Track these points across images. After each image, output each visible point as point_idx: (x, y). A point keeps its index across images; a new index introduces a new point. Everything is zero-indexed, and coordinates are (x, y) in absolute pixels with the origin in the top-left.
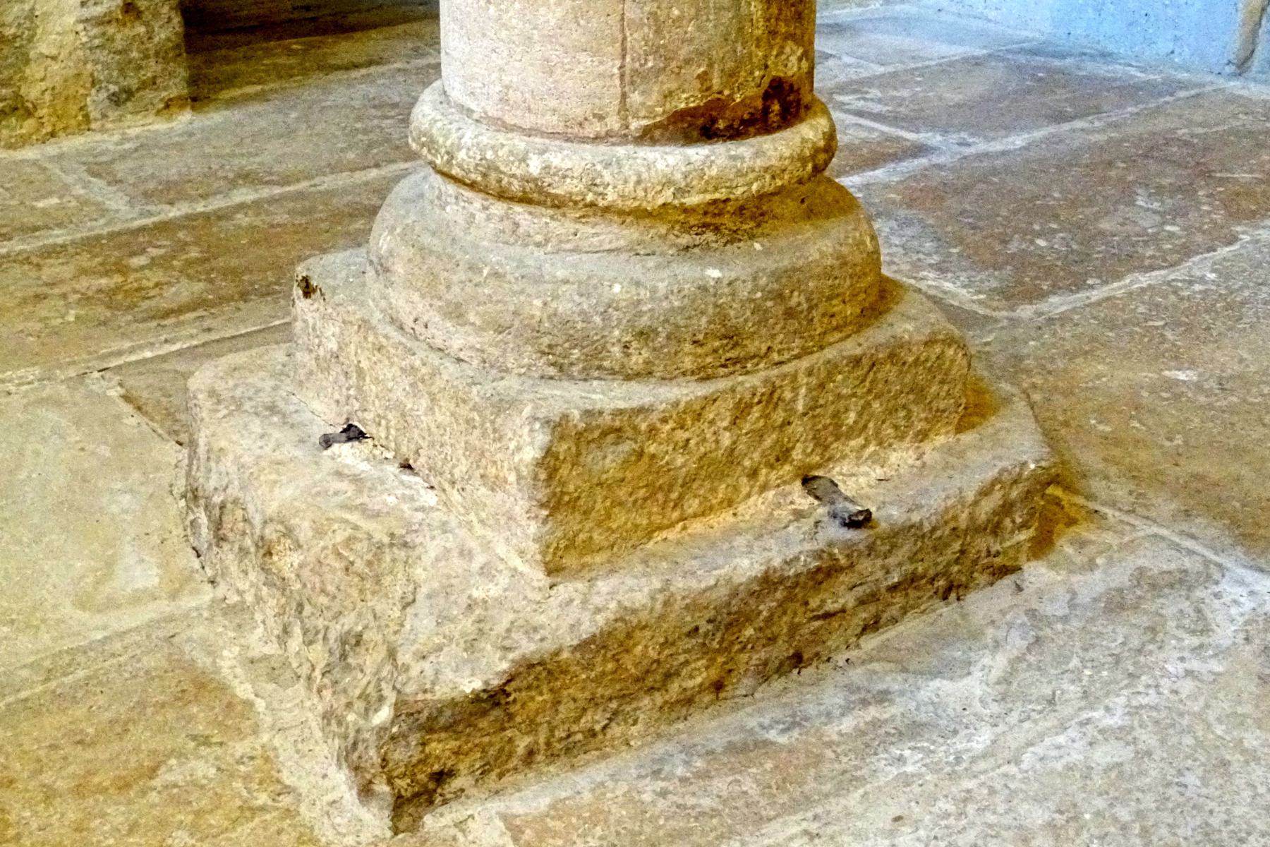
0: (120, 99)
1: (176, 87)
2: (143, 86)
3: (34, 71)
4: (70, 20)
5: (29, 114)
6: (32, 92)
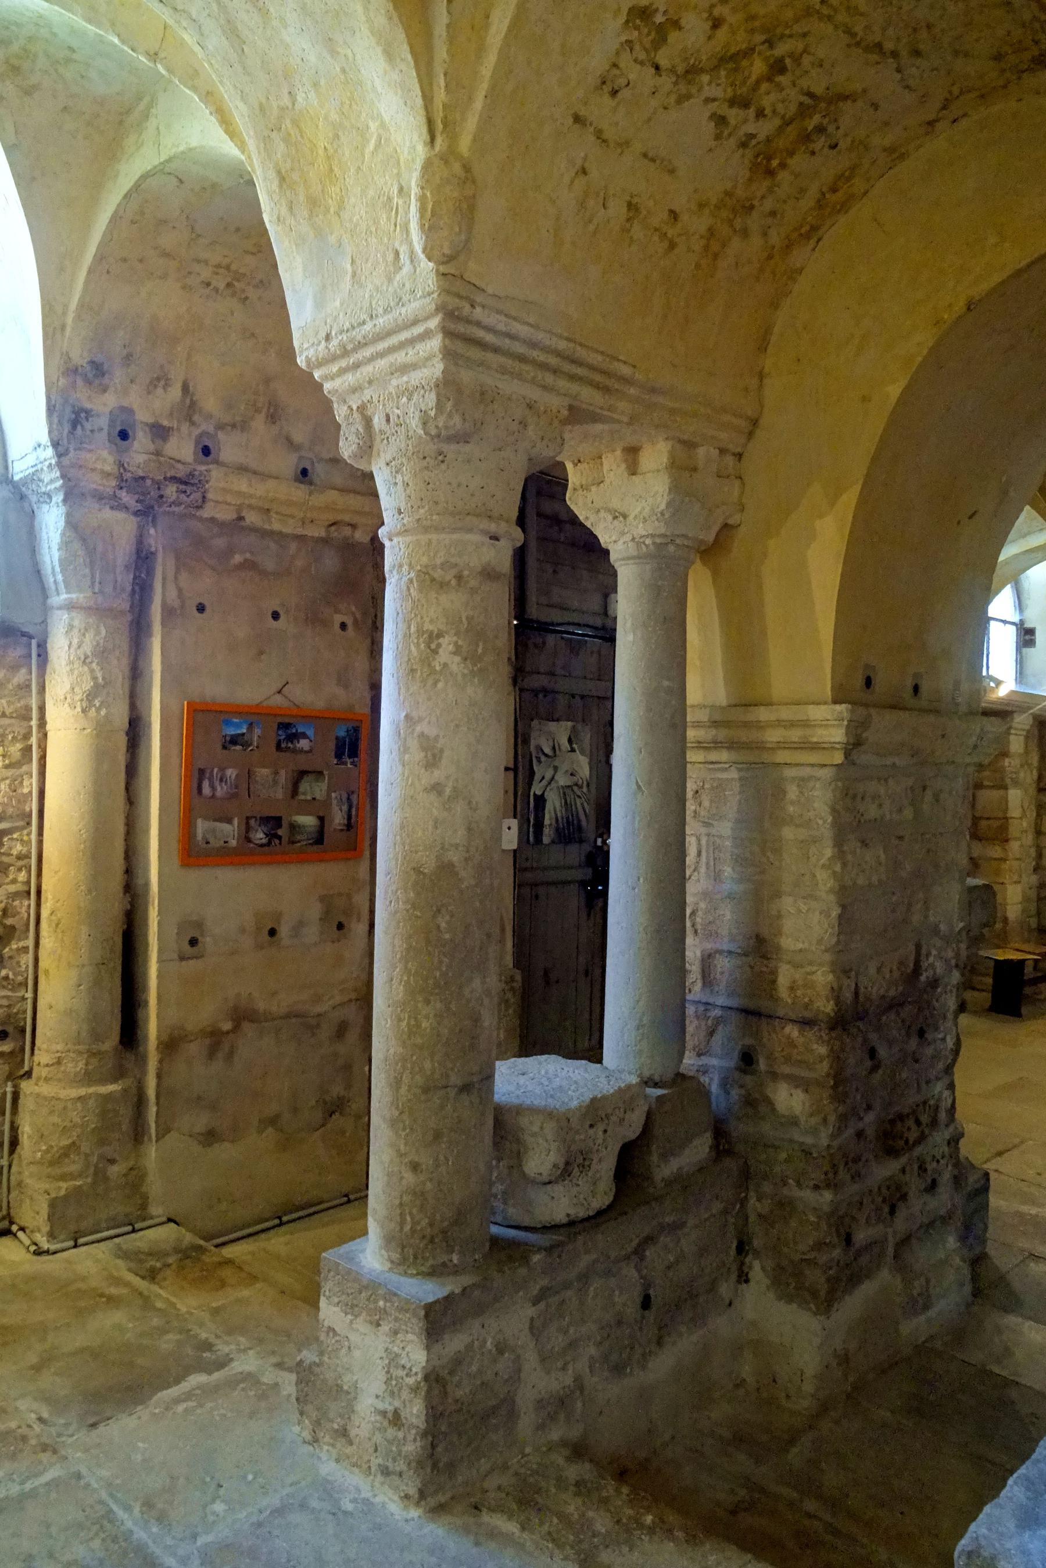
0: (386, 1472)
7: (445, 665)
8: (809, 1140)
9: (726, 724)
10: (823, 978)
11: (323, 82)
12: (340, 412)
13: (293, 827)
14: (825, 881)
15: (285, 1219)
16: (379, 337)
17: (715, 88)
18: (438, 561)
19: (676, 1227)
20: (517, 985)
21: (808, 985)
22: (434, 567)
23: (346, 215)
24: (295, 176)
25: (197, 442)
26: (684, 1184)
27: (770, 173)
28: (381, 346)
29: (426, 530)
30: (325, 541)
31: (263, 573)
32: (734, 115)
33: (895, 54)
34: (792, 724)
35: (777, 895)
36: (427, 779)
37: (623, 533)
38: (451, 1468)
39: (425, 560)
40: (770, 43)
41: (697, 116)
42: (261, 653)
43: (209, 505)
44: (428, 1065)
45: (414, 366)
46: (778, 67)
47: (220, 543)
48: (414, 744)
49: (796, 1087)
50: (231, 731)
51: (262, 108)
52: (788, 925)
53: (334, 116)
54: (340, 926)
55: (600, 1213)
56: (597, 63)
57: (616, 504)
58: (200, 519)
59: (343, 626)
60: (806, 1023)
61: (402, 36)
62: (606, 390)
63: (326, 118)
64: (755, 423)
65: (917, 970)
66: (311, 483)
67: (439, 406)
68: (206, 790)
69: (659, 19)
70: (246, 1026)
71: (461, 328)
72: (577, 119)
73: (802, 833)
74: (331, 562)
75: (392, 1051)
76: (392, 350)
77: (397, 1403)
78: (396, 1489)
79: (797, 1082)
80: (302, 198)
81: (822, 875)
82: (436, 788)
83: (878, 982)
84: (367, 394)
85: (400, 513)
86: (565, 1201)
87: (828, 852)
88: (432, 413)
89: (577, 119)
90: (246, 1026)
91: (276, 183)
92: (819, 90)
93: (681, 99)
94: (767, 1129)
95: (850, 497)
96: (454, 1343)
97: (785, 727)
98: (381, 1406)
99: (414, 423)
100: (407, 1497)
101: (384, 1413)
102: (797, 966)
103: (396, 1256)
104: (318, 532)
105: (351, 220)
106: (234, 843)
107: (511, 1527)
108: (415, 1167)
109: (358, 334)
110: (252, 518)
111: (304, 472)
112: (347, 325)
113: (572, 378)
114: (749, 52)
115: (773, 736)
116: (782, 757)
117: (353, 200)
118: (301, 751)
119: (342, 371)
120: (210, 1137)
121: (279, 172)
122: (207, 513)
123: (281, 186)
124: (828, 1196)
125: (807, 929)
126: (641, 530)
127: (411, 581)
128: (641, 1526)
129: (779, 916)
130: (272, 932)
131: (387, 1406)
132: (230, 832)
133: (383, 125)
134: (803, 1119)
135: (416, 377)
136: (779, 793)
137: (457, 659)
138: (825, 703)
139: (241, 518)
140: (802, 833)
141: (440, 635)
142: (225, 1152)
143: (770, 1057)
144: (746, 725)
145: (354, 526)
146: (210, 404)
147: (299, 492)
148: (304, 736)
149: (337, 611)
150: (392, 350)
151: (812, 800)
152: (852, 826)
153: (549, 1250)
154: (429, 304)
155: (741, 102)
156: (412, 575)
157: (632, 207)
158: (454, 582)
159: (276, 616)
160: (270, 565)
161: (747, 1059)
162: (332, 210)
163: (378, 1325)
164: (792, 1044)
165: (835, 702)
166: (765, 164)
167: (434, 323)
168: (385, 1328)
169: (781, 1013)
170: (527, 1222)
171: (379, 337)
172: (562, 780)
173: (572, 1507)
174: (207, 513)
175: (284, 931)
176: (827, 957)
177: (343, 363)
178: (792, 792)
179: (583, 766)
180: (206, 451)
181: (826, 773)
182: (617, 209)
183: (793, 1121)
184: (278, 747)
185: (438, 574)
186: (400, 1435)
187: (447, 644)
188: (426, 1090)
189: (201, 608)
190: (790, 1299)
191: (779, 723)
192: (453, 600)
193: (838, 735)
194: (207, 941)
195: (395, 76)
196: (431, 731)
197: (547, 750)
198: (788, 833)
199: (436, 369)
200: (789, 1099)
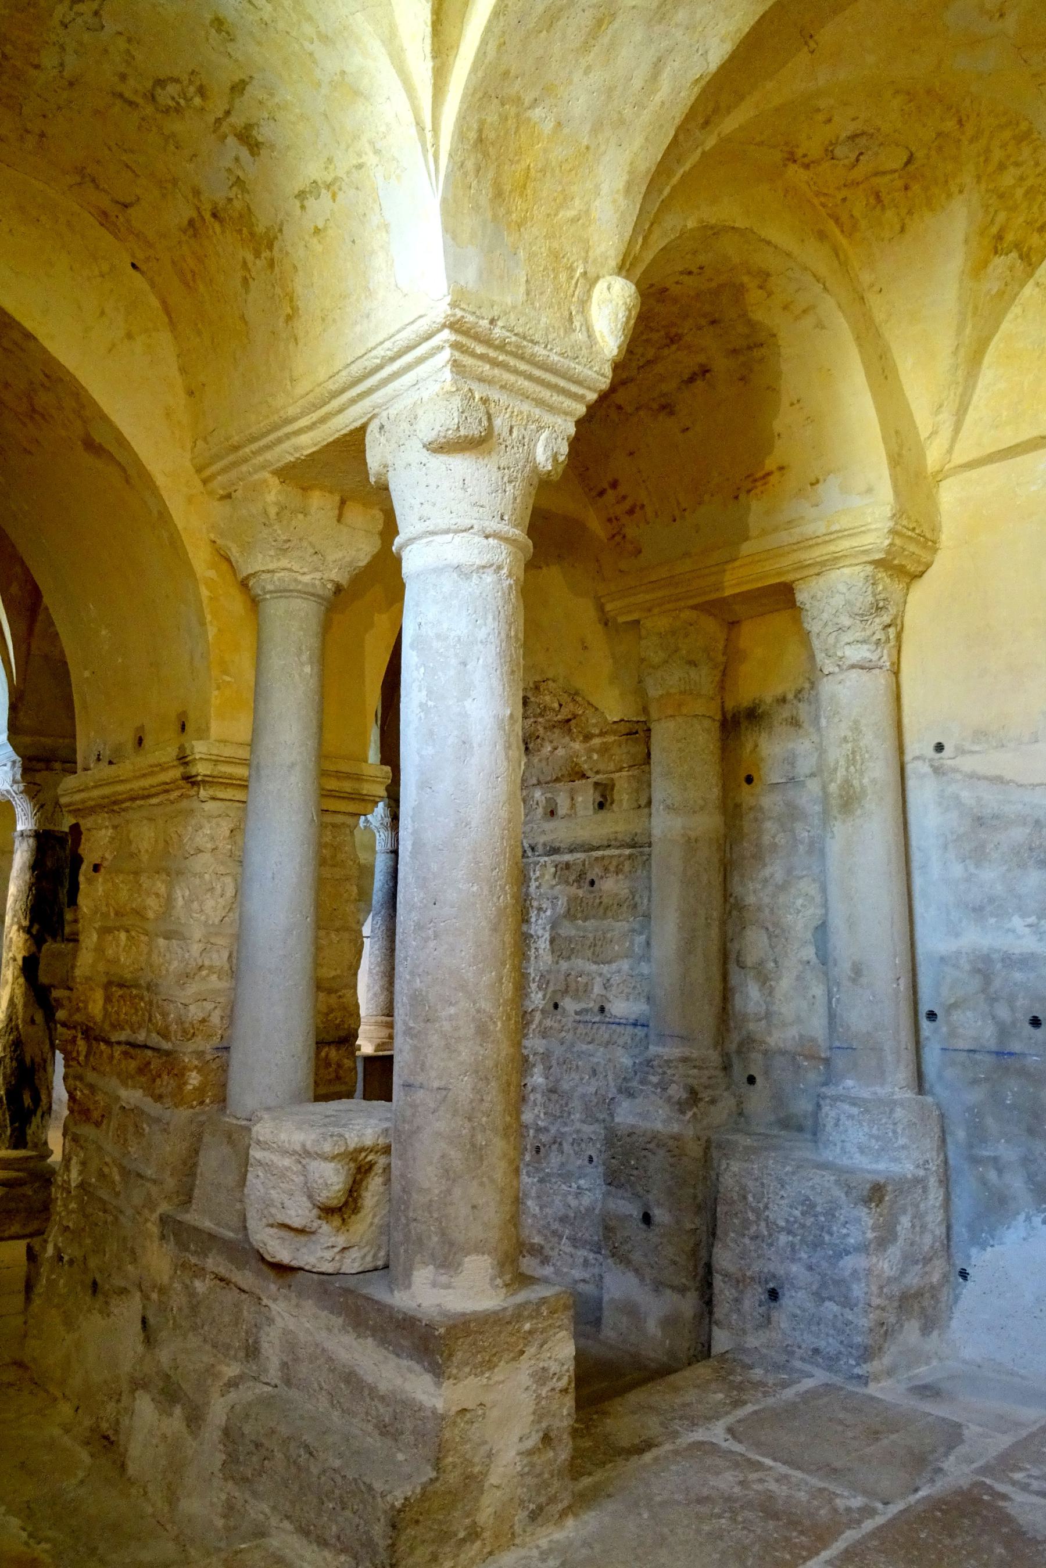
11: (566, 131)
34: (348, 776)
37: (317, 570)
51: (506, 74)
63: (545, 151)
75: (503, 1054)
84: (494, 394)
91: (473, 135)
97: (338, 778)
101: (530, 1453)
109: (530, 349)
117: (535, 231)
119: (482, 357)
121: (480, 131)
127: (510, 586)
133: (587, 212)
163: (522, 1352)
177: (492, 354)
195: (622, 202)
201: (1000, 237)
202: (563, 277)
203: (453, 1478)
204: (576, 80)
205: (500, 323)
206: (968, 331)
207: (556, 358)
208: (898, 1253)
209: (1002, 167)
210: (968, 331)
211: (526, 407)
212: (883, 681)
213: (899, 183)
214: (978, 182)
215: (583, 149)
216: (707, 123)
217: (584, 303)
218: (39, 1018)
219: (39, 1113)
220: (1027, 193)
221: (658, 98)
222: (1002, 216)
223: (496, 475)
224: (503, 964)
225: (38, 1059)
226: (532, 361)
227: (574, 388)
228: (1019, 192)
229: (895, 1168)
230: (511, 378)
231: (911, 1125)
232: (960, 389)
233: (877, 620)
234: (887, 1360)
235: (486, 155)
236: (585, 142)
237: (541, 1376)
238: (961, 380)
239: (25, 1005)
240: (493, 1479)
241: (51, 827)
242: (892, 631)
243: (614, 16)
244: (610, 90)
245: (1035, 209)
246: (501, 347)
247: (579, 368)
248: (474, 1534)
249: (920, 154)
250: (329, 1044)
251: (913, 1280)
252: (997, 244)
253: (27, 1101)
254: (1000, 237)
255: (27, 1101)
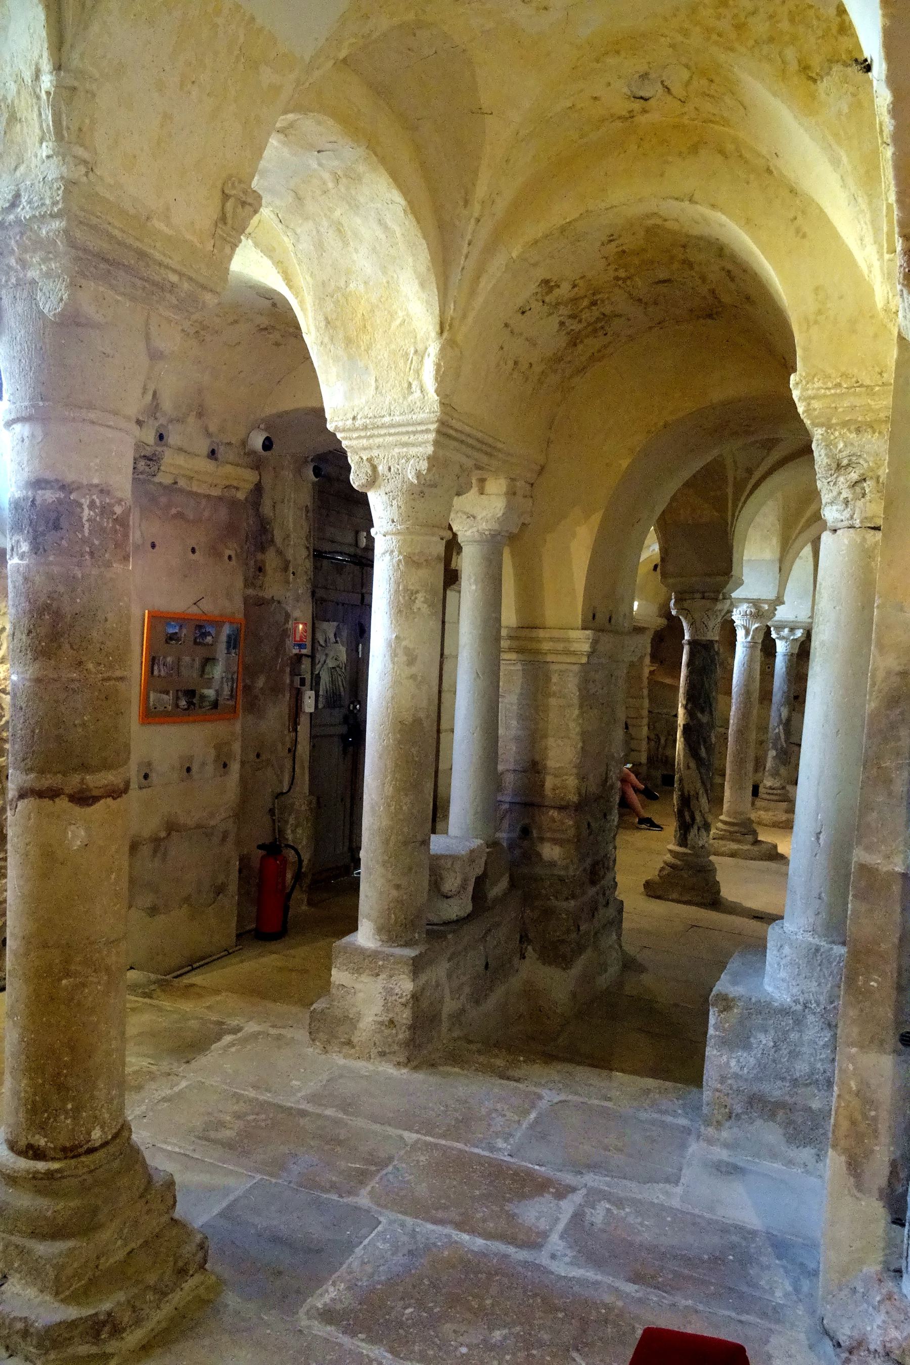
0: (382, 1054)
1: (402, 1059)
2: (389, 1053)
3: (357, 1033)
4: (371, 1019)
5: (353, 1047)
6: (355, 1040)
7: (419, 609)
8: (562, 873)
9: (517, 638)
10: (572, 782)
11: (371, 283)
12: (352, 460)
13: (203, 697)
14: (574, 729)
15: (195, 966)
16: (392, 426)
17: (564, 311)
18: (417, 551)
19: (498, 925)
20: (314, 805)
21: (565, 787)
22: (414, 554)
23: (373, 353)
24: (338, 323)
25: (157, 431)
26: (501, 900)
27: (575, 345)
28: (392, 431)
29: (411, 533)
30: (220, 498)
31: (188, 521)
32: (568, 322)
33: (646, 303)
35: (545, 736)
36: (408, 671)
38: (419, 1047)
39: (409, 550)
40: (594, 294)
41: (554, 321)
42: (186, 576)
43: (160, 474)
44: (406, 830)
45: (413, 445)
46: (594, 303)
47: (163, 500)
48: (400, 652)
49: (555, 844)
50: (171, 631)
51: (323, 283)
52: (551, 754)
53: (374, 300)
54: (225, 765)
55: (469, 915)
56: (520, 301)
57: (468, 509)
58: (154, 484)
59: (230, 558)
60: (561, 808)
61: (433, 278)
62: (490, 455)
64: (543, 468)
65: (606, 781)
66: (216, 459)
67: (429, 470)
68: (156, 673)
69: (552, 284)
70: (174, 833)
71: (445, 430)
72: (506, 325)
73: (562, 702)
74: (223, 514)
76: (398, 434)
77: (391, 1016)
78: (390, 1061)
79: (555, 841)
80: (341, 336)
81: (572, 725)
82: (413, 677)
83: (593, 787)
84: (375, 453)
85: (393, 521)
86: (456, 908)
87: (577, 712)
88: (424, 473)
89: (506, 325)
90: (174, 833)
91: (323, 324)
92: (607, 312)
93: (550, 314)
94: (539, 870)
95: (596, 518)
96: (423, 978)
98: (380, 1019)
99: (411, 476)
100: (399, 1063)
102: (556, 776)
103: (385, 938)
104: (216, 492)
105: (376, 357)
106: (170, 708)
107: (457, 1070)
108: (398, 887)
109: (379, 422)
110: (182, 483)
111: (213, 452)
112: (371, 415)
113: (479, 450)
114: (582, 298)
115: (546, 646)
116: (549, 658)
117: (379, 346)
118: (208, 644)
120: (153, 911)
121: (326, 319)
122: (156, 479)
123: (326, 326)
124: (573, 903)
125: (562, 756)
126: (484, 526)
127: (400, 561)
128: (519, 1061)
129: (546, 748)
130: (189, 770)
131: (385, 1018)
132: (168, 699)
133: (408, 315)
134: (559, 863)
135: (413, 451)
136: (548, 679)
137: (426, 606)
138: (578, 629)
139: (176, 483)
140: (562, 702)
141: (417, 592)
142: (161, 919)
143: (540, 828)
144: (532, 639)
145: (237, 489)
146: (167, 405)
147: (208, 466)
148: (209, 634)
149: (227, 548)
150: (398, 434)
151: (566, 684)
152: (587, 699)
153: (454, 932)
154: (433, 417)
155: (573, 317)
156: (401, 557)
157: (516, 363)
158: (425, 563)
159: (193, 551)
160: (191, 516)
161: (525, 832)
162: (362, 348)
164: (553, 820)
165: (584, 628)
166: (574, 341)
167: (433, 427)
168: (383, 976)
169: (546, 804)
170: (436, 921)
171: (392, 426)
172: (331, 664)
173: (481, 1059)
174: (156, 479)
175: (195, 769)
176: (575, 771)
177: (363, 434)
178: (555, 679)
179: (342, 652)
180: (161, 437)
181: (576, 668)
182: (511, 363)
183: (553, 864)
184: (195, 643)
185: (415, 558)
186: (394, 1031)
187: (420, 597)
188: (405, 843)
189: (153, 546)
190: (550, 964)
191: (551, 639)
192: (423, 573)
193: (586, 647)
194: (153, 776)
196: (411, 646)
197: (322, 642)
198: (553, 701)
199: (430, 450)
200: (550, 852)
201: (805, 69)
202: (401, 363)
203: (338, 1013)
204: (355, 258)
205: (359, 417)
206: (845, 159)
207: (401, 418)
208: (752, 1061)
209: (740, 27)
210: (845, 159)
211: (397, 450)
212: (846, 542)
213: (704, 82)
214: (732, 50)
215: (386, 285)
216: (466, 203)
217: (418, 372)
218: (693, 765)
219: (696, 827)
220: (792, 20)
221: (398, 235)
222: (790, 54)
223: (385, 498)
224: (387, 777)
225: (692, 793)
226: (383, 426)
227: (419, 428)
228: (785, 25)
229: (776, 995)
230: (381, 440)
231: (792, 963)
232: (868, 216)
233: (842, 479)
234: (725, 1134)
235: (335, 328)
236: (385, 281)
237: (389, 992)
238: (864, 206)
239: (684, 756)
240: (361, 1025)
241: (696, 638)
242: (868, 486)
243: (340, 223)
244: (374, 249)
245: (815, 22)
246: (365, 428)
247: (414, 417)
248: (349, 1043)
249: (684, 60)
250: (554, 808)
251: (776, 1091)
252: (808, 74)
253: (688, 818)
254: (805, 69)
255: (688, 818)
